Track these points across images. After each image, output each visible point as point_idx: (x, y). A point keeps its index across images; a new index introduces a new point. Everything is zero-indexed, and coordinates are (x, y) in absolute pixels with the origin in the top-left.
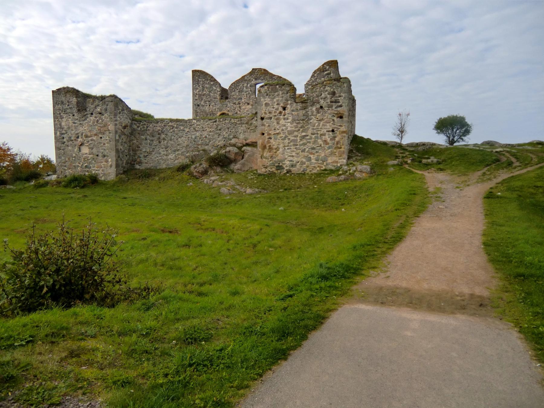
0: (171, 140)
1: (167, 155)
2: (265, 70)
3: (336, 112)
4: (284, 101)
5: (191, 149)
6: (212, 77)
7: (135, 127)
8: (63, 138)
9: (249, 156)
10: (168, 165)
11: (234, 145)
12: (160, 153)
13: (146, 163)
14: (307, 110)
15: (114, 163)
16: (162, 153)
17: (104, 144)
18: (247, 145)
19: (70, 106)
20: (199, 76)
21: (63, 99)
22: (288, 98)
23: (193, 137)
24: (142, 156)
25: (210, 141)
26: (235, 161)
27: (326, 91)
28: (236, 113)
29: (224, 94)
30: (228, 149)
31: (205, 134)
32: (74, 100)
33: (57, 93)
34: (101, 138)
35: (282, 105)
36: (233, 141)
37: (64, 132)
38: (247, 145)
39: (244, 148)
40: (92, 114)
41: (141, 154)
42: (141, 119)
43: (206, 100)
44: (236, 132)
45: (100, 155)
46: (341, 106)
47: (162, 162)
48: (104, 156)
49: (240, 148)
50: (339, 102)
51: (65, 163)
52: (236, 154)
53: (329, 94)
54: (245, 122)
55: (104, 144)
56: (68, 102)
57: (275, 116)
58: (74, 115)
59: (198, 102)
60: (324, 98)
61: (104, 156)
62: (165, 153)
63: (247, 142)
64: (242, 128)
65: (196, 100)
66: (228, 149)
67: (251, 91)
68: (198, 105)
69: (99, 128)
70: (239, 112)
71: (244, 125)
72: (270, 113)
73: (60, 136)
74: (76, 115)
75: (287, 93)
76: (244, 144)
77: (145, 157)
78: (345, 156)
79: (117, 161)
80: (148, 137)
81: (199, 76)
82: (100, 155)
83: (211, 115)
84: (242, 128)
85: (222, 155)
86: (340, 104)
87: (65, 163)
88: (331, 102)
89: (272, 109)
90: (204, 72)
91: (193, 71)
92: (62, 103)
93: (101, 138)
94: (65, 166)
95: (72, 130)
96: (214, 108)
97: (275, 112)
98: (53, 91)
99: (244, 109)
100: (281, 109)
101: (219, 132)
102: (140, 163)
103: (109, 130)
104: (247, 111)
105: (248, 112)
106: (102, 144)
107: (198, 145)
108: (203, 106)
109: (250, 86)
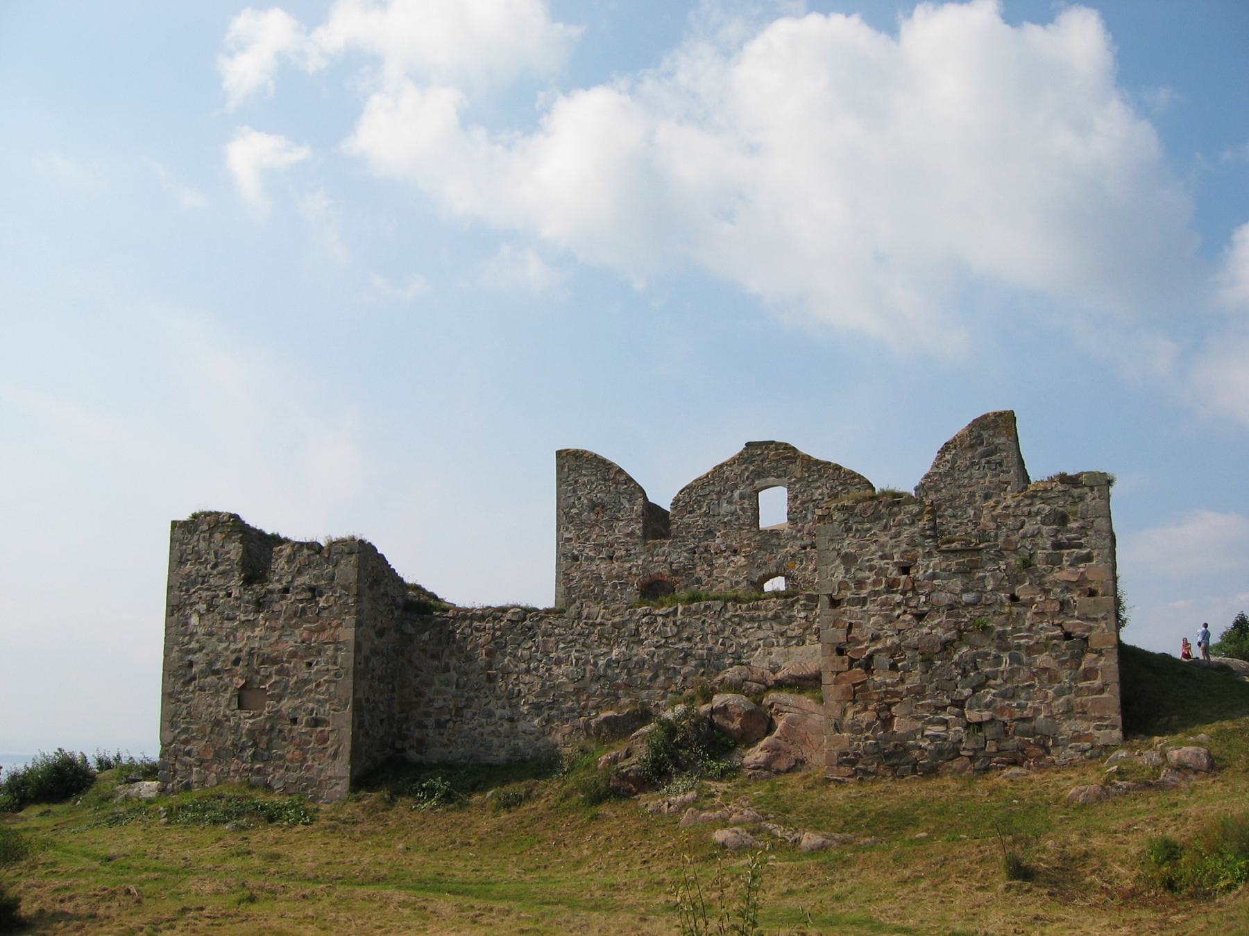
0: (528, 671)
1: (511, 720)
2: (787, 447)
3: (1074, 579)
4: (904, 546)
6: (621, 471)
7: (409, 629)
8: (191, 664)
9: (791, 722)
10: (516, 750)
11: (736, 687)
12: (490, 714)
13: (445, 746)
15: (347, 744)
16: (498, 712)
17: (318, 685)
18: (780, 685)
19: (221, 568)
20: (577, 468)
24: (430, 722)
26: (747, 739)
27: (1038, 513)
29: (656, 522)
30: (718, 700)
31: (642, 652)
32: (234, 550)
33: (184, 531)
34: (309, 665)
36: (732, 673)
37: (193, 645)
38: (780, 685)
39: (773, 695)
40: (286, 590)
41: (427, 715)
42: (420, 607)
44: (743, 647)
45: (303, 718)
46: (1088, 558)
47: (496, 741)
48: (316, 722)
49: (757, 697)
50: (1080, 546)
51: (186, 742)
52: (749, 715)
53: (1043, 523)
54: (770, 614)
55: (318, 685)
57: (877, 593)
58: (229, 595)
59: (575, 547)
60: (1033, 536)
61: (316, 722)
62: (507, 712)
63: (779, 675)
64: (761, 634)
65: (570, 540)
66: (718, 700)
67: (743, 509)
68: (576, 558)
71: (766, 626)
72: (860, 584)
73: (181, 659)
74: (235, 593)
75: (913, 523)
76: (770, 683)
77: (440, 725)
78: (1117, 718)
79: (355, 737)
80: (453, 662)
81: (577, 468)
82: (303, 718)
83: (615, 586)
84: (761, 634)
85: (701, 719)
86: (1085, 551)
87: (186, 742)
88: (1058, 546)
89: (867, 574)
90: (596, 456)
91: (559, 453)
94: (189, 753)
95: (220, 641)
96: (628, 565)
97: (875, 583)
98: (174, 523)
99: (723, 567)
100: (893, 573)
101: (685, 644)
102: (421, 744)
103: (335, 642)
105: (735, 579)
107: (618, 687)
108: (590, 559)
109: (742, 497)
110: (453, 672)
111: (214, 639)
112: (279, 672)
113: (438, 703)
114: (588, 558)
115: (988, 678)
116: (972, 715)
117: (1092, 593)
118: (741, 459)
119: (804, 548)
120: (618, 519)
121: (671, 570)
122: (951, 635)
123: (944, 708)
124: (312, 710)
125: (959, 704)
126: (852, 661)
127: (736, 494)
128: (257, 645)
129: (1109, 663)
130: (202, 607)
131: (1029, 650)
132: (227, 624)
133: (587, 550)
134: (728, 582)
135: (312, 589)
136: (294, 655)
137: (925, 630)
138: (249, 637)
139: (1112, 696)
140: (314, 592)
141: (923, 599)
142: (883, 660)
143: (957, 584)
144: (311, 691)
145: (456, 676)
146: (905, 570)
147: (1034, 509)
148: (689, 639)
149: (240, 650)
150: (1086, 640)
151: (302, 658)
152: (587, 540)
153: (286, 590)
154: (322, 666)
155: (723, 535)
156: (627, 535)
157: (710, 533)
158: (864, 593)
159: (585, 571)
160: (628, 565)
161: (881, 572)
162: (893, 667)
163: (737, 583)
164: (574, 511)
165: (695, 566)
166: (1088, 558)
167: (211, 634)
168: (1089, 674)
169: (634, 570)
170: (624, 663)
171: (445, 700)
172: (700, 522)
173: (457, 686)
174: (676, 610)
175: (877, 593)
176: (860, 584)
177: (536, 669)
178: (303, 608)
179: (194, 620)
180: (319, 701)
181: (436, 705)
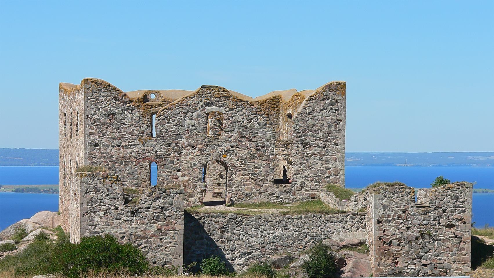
4: (404, 204)
5: (267, 252)
14: (430, 214)
19: (111, 196)
21: (99, 186)
22: (409, 201)
23: (271, 236)
25: (294, 242)
28: (172, 162)
31: (288, 233)
34: (161, 239)
35: (402, 207)
40: (148, 208)
43: (113, 135)
46: (464, 211)
50: (462, 207)
54: (339, 220)
56: (108, 190)
57: (394, 219)
58: (117, 209)
63: (344, 243)
65: (92, 134)
68: (96, 145)
69: (159, 227)
70: (175, 160)
72: (389, 216)
78: (470, 264)
83: (121, 163)
86: (463, 209)
88: (455, 207)
89: (391, 212)
92: (97, 190)
93: (161, 239)
96: (129, 151)
97: (394, 216)
100: (400, 213)
104: (193, 159)
106: (163, 248)
109: (198, 116)
110: (205, 239)
111: (109, 228)
112: (145, 243)
113: (199, 252)
114: (104, 146)
115: (430, 250)
116: (424, 262)
117: (465, 223)
118: (199, 95)
119: (232, 147)
120: (124, 124)
121: (156, 155)
122: (418, 235)
123: (415, 259)
124: (164, 258)
125: (420, 258)
126: (385, 242)
127: (195, 114)
128: (134, 231)
129: (468, 246)
130: (102, 213)
131: (444, 241)
132: (115, 221)
133: (104, 141)
134: (189, 164)
135: (162, 208)
136: (154, 235)
137: (410, 233)
138: (129, 227)
139: (468, 257)
140: (162, 209)
141: (410, 222)
142: (395, 242)
143: (421, 218)
144: (162, 250)
145: (206, 241)
146: (404, 212)
147: (448, 193)
148: (308, 229)
149: (125, 233)
150: (462, 238)
151: (158, 237)
152: (104, 135)
153: (148, 208)
154: (168, 240)
155: (186, 137)
156: (129, 133)
157: (179, 135)
158: (389, 219)
159: (102, 153)
160: (129, 151)
161: (396, 212)
162: (399, 245)
163: (195, 165)
164: (95, 117)
165: (170, 153)
166: (464, 211)
167: (108, 225)
168: (462, 249)
169: (133, 154)
170: (280, 237)
171: (201, 251)
172: (174, 129)
173: (207, 245)
174: (302, 217)
175: (394, 219)
176: (389, 216)
177: (242, 239)
178: (158, 216)
179: (97, 219)
180: (167, 254)
181: (197, 253)
